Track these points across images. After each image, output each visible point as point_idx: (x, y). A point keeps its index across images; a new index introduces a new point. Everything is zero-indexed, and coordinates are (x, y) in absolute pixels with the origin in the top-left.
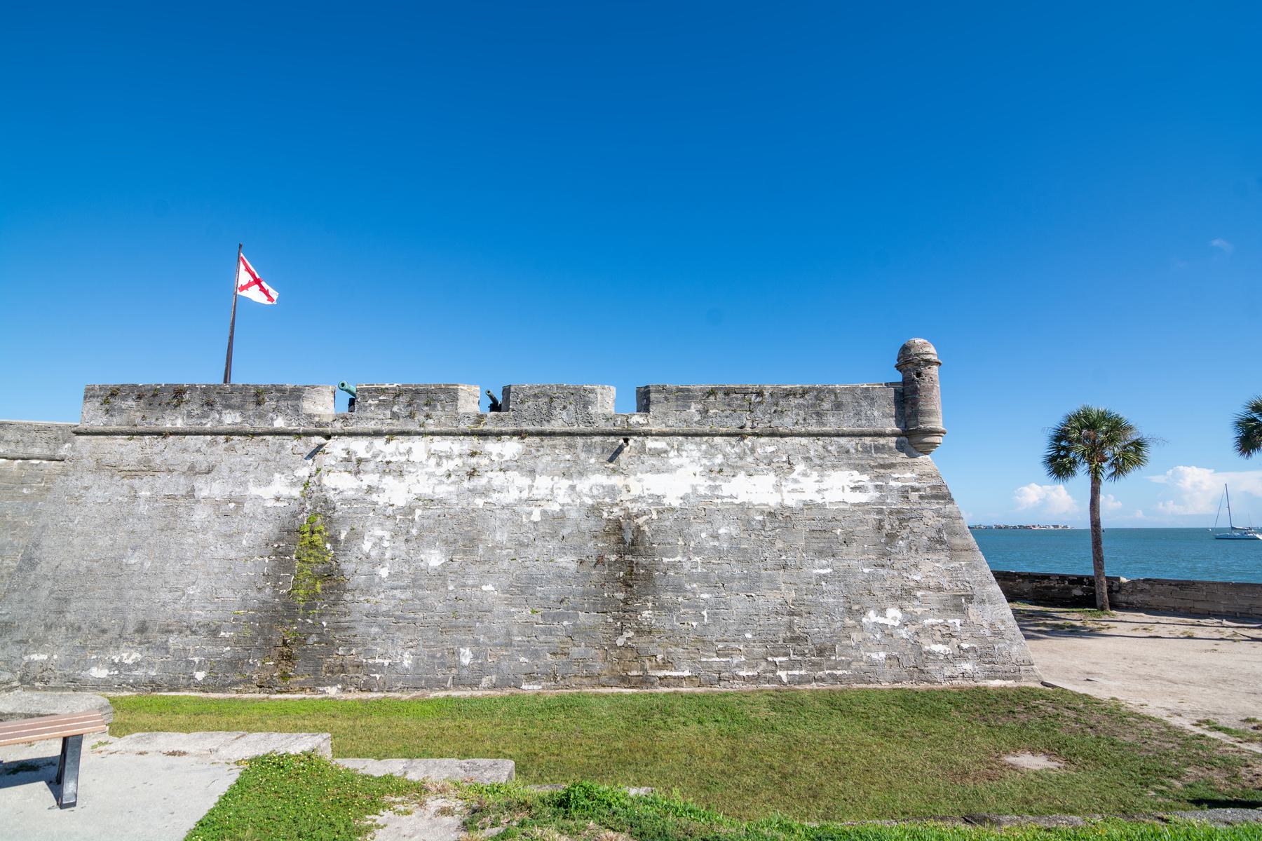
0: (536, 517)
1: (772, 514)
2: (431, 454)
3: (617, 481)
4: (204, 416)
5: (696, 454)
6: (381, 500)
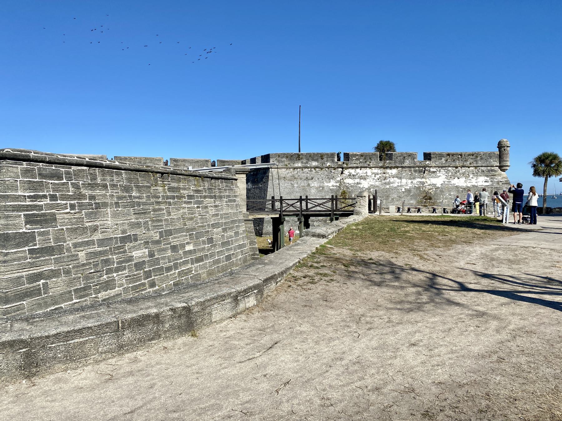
0: (403, 190)
1: (464, 189)
2: (372, 173)
3: (423, 180)
4: (307, 163)
5: (444, 173)
6: (361, 186)
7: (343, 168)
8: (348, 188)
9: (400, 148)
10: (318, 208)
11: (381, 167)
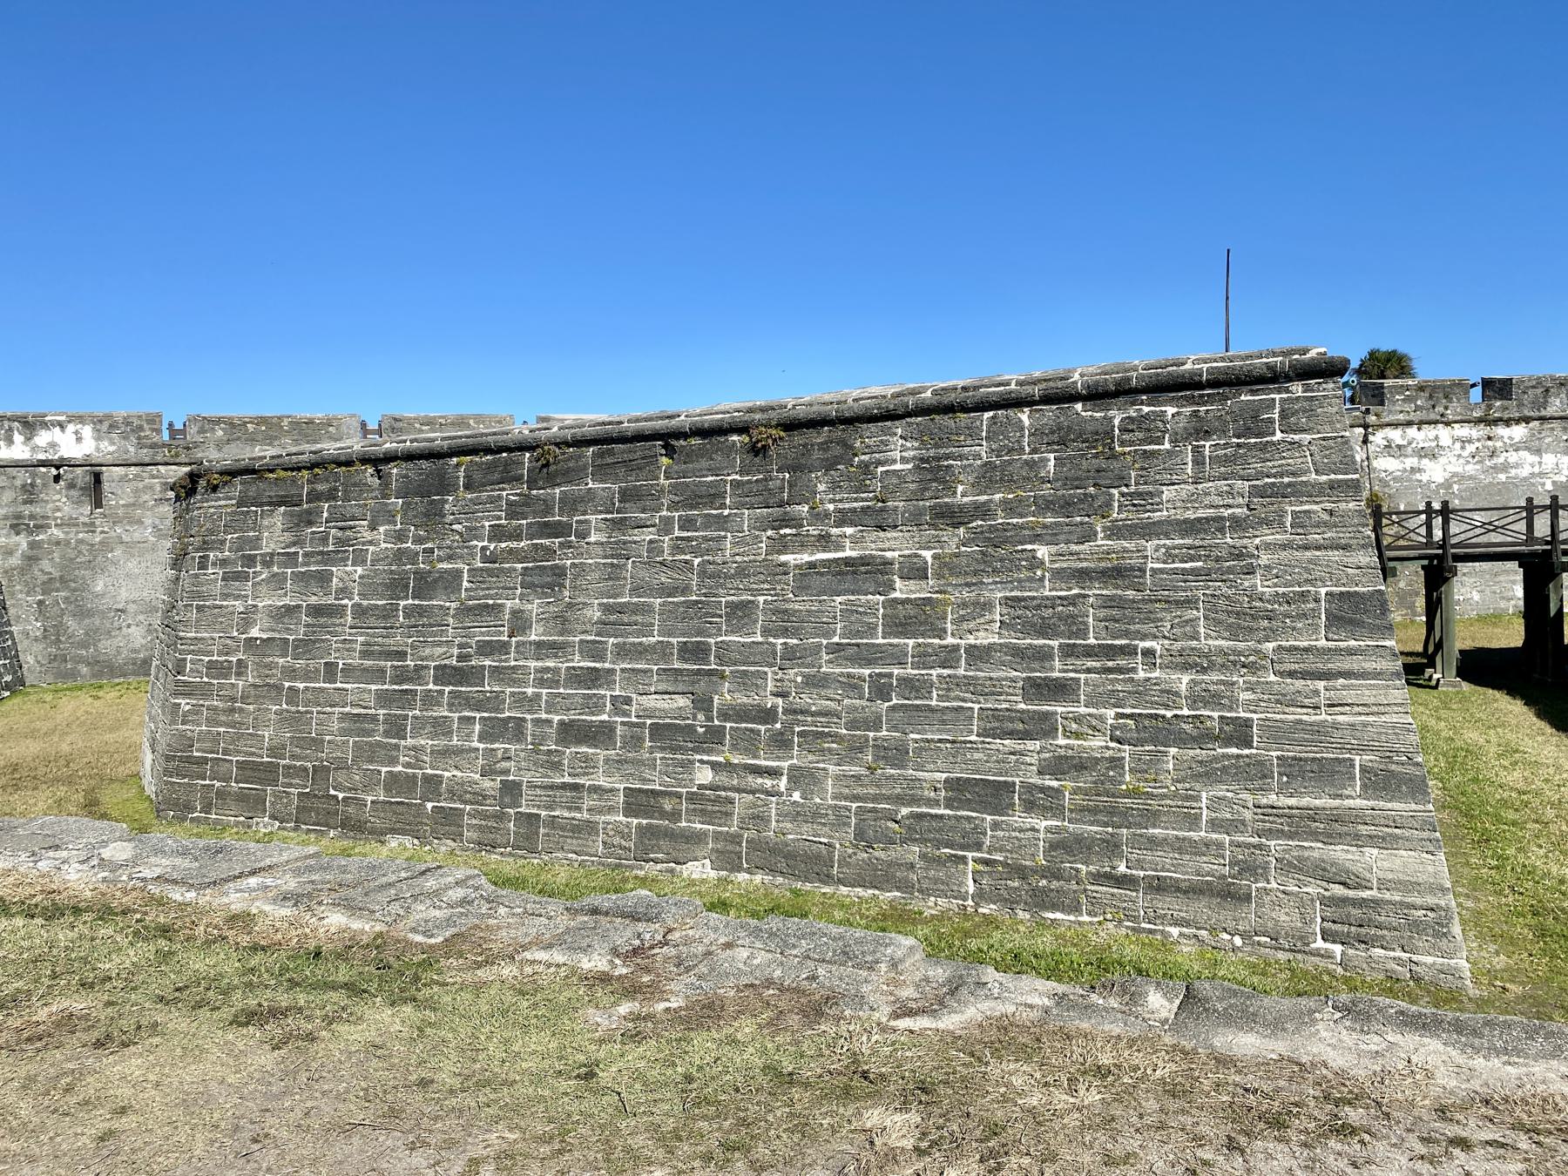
6: (1424, 478)
7: (1366, 426)
8: (1385, 484)
9: (1426, 370)
10: (1494, 538)
11: (1479, 421)
